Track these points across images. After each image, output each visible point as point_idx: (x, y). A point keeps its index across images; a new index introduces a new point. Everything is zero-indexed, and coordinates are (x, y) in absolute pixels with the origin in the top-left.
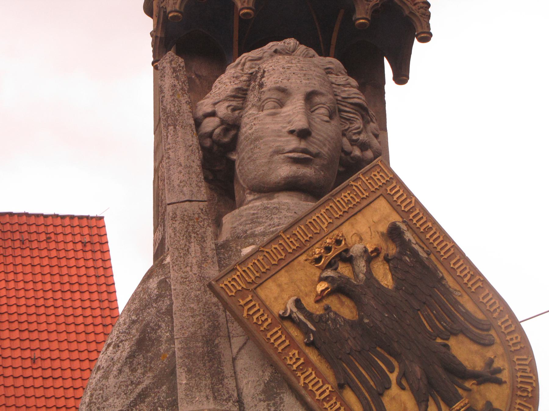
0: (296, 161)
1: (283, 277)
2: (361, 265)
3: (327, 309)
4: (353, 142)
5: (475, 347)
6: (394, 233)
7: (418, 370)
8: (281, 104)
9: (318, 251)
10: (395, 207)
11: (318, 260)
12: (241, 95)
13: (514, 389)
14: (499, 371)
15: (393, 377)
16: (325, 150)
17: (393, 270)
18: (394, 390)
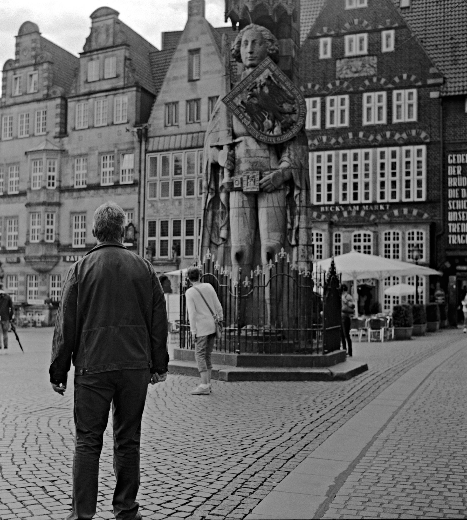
0: (250, 60)
1: (239, 96)
2: (259, 89)
3: (251, 102)
4: (270, 50)
5: (289, 105)
6: (269, 78)
7: (271, 114)
8: (247, 44)
9: (248, 87)
10: (271, 70)
11: (248, 90)
12: (239, 42)
13: (299, 114)
14: (296, 110)
15: (266, 117)
16: (258, 55)
17: (269, 88)
18: (267, 120)
